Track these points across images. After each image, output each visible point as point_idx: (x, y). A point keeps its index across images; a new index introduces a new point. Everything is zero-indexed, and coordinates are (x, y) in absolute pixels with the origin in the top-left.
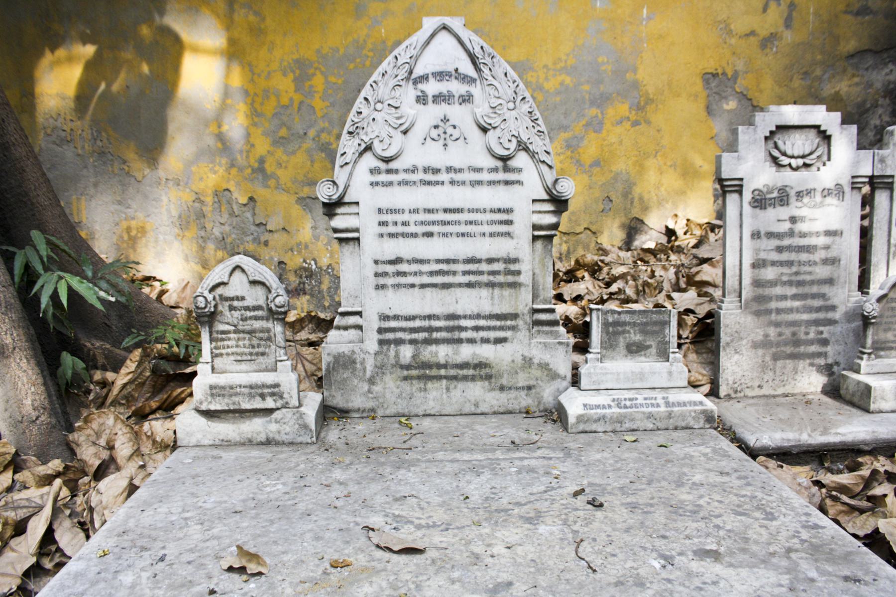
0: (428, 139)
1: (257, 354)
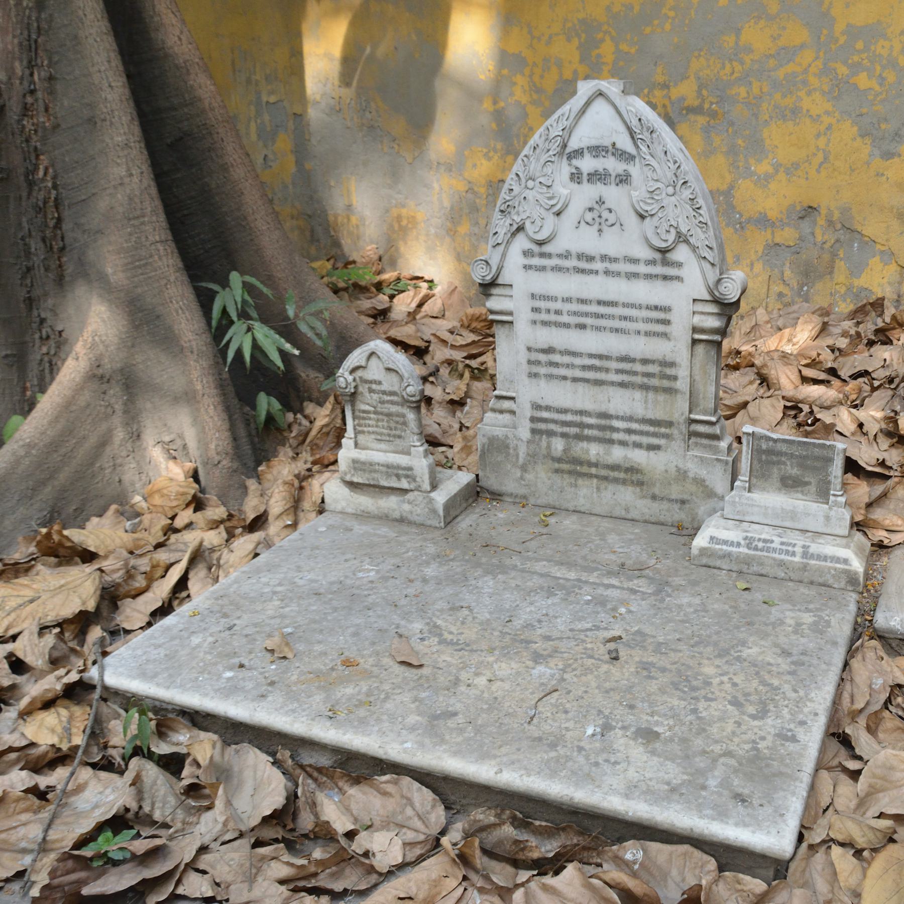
0: (582, 223)
1: (394, 436)
